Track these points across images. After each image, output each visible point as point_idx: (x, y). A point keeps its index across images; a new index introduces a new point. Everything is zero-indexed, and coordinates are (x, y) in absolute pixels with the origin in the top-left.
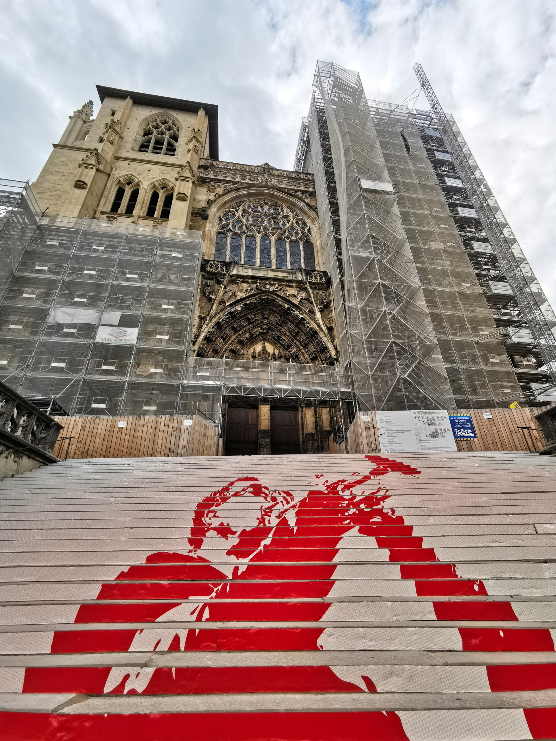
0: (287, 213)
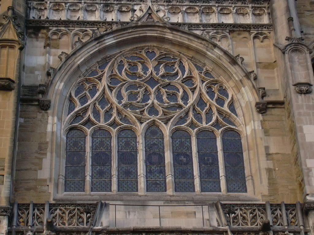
0: (190, 71)
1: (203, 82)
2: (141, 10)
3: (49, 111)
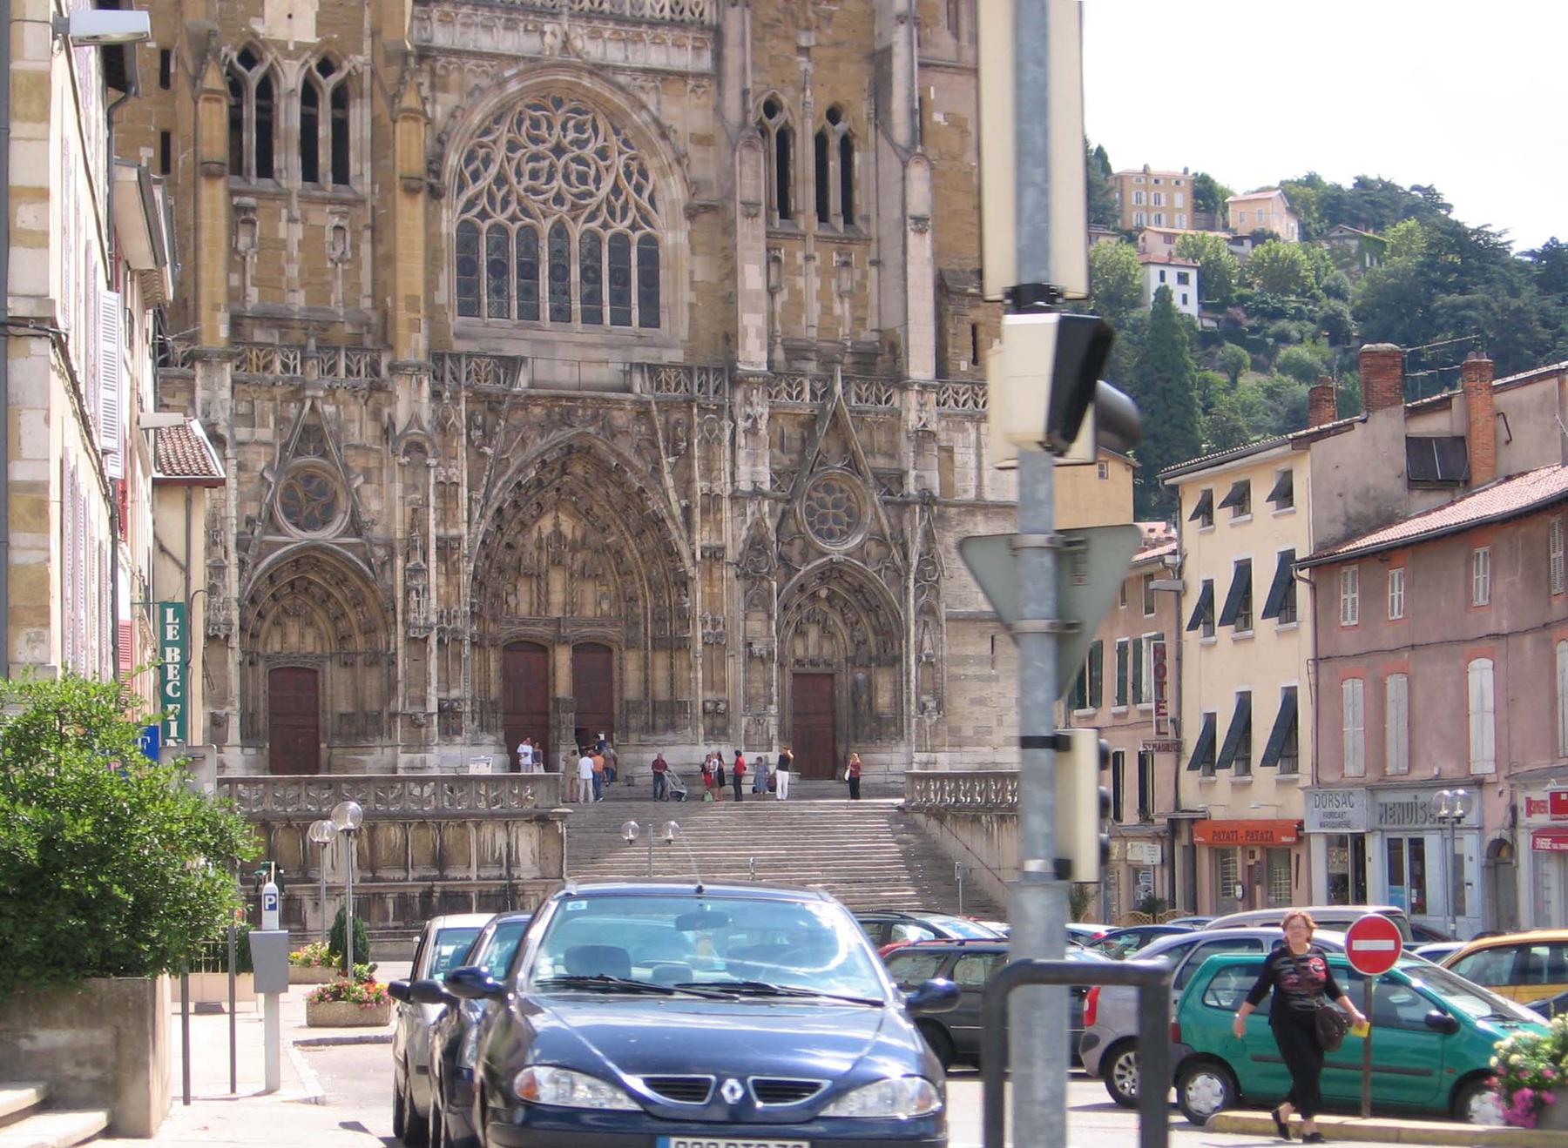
1: (620, 153)
2: (554, 34)
3: (444, 201)
